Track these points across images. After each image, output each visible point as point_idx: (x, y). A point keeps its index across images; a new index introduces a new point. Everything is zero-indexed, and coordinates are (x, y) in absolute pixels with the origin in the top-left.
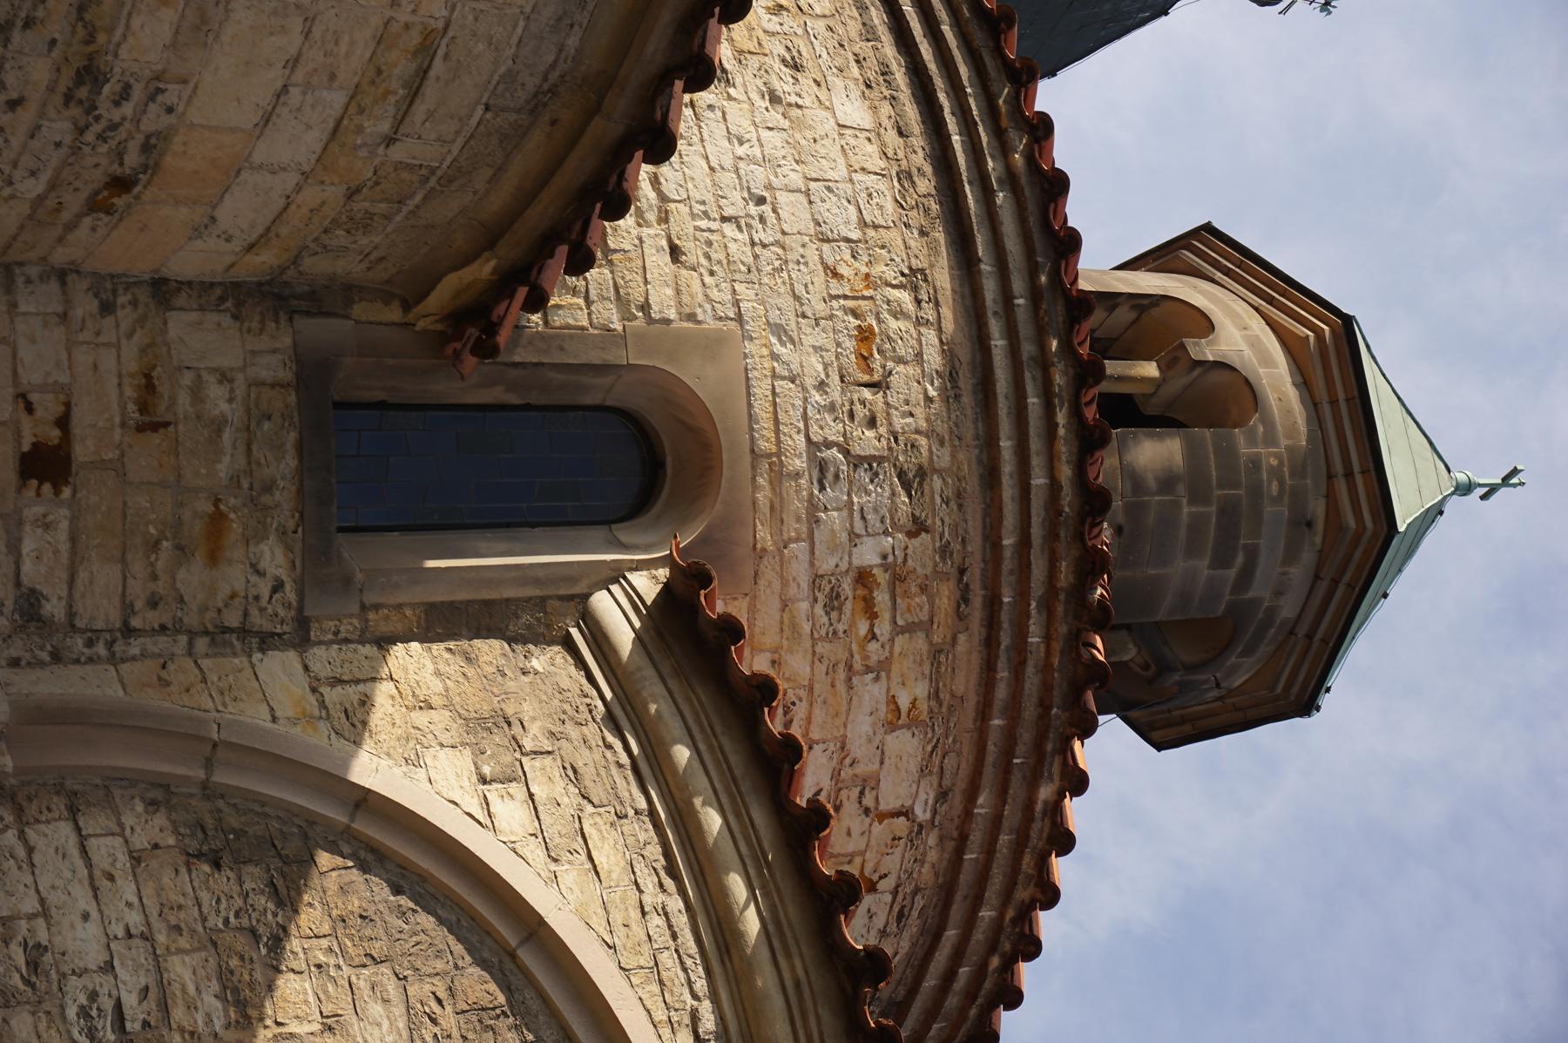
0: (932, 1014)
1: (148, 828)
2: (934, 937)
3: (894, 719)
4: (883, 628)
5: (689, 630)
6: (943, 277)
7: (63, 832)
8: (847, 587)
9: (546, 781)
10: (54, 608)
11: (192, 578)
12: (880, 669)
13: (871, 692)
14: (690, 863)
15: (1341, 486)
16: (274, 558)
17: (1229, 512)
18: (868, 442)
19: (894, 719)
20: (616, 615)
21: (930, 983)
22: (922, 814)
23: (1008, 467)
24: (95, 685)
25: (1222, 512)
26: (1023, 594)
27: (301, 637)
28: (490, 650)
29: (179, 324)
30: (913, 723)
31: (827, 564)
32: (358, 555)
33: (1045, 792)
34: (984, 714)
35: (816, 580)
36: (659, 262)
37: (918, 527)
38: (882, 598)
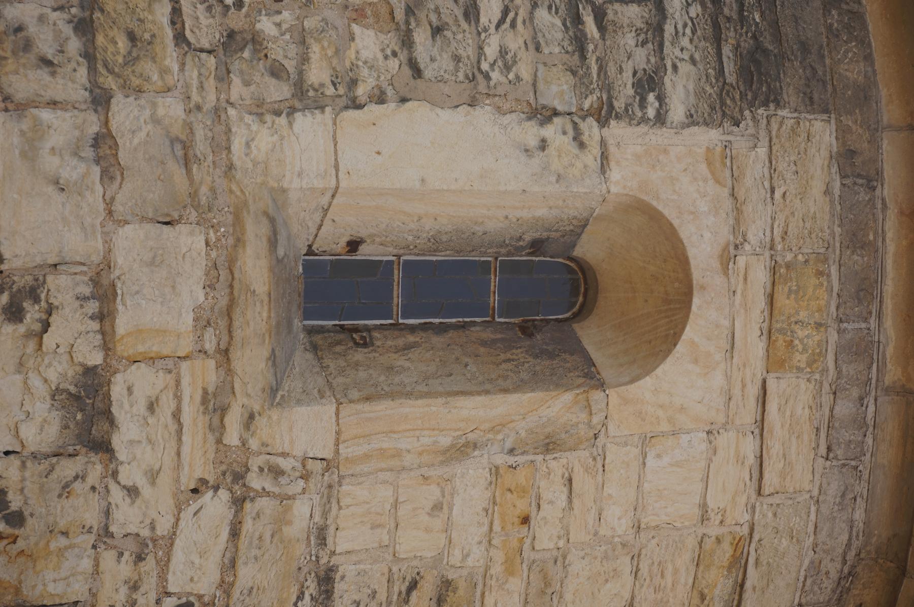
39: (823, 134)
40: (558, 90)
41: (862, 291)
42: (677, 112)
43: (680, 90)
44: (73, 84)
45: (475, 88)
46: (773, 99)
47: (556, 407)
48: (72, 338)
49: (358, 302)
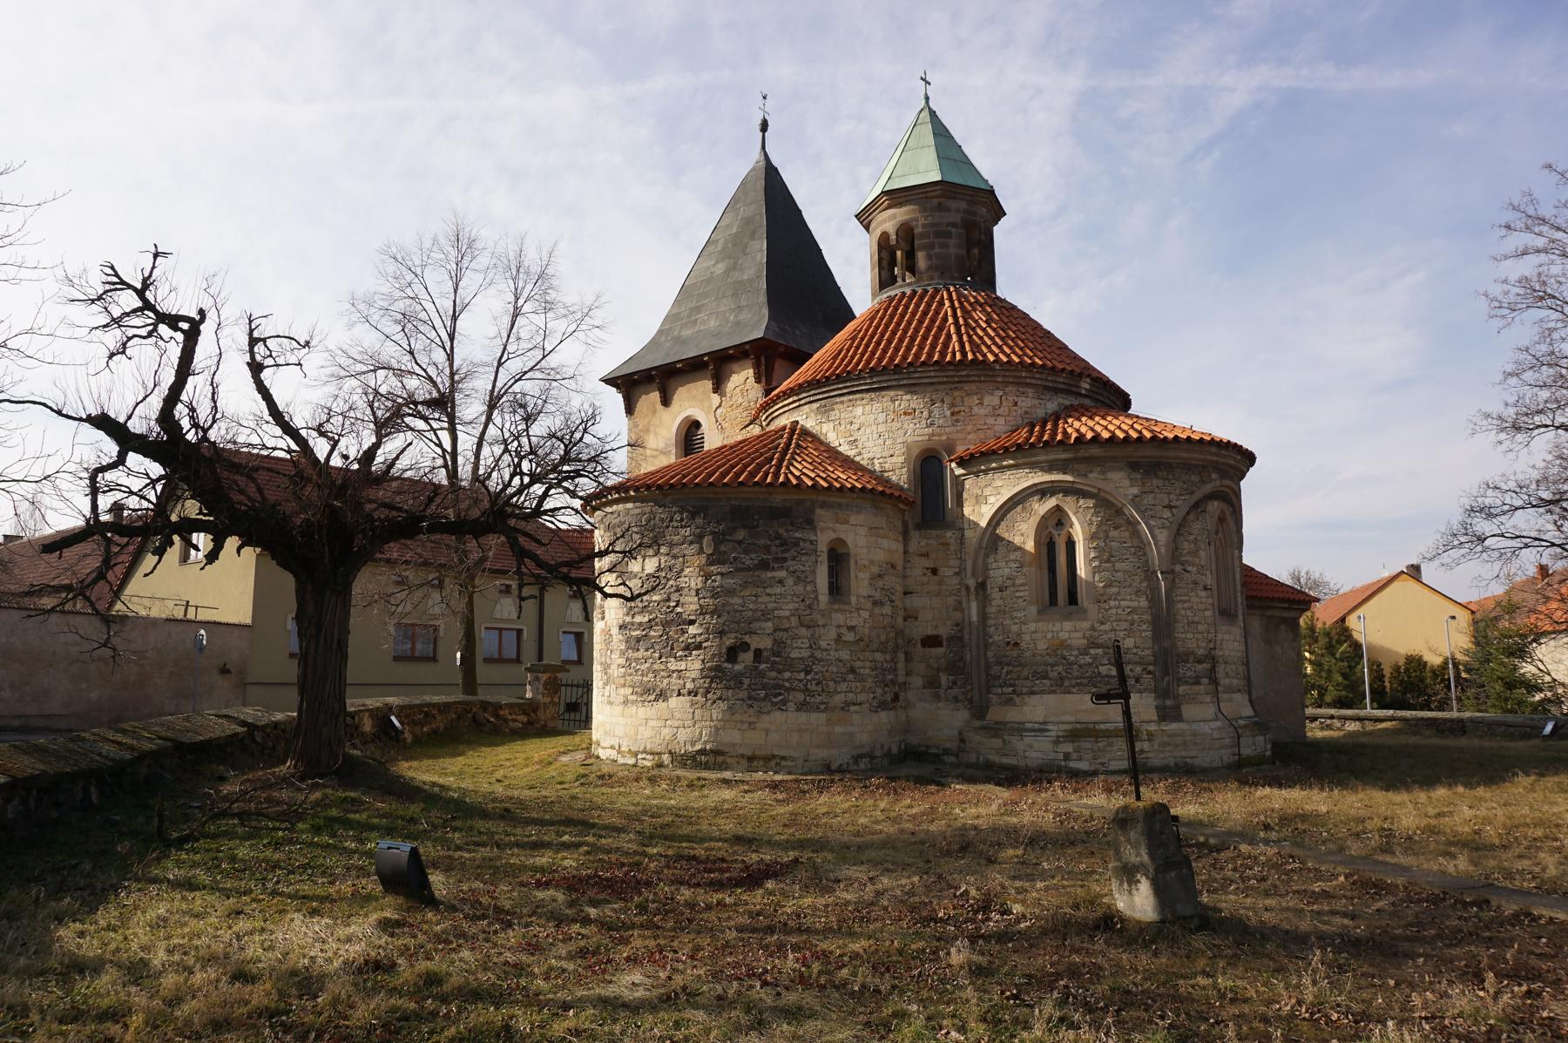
1: (991, 559)
3: (981, 404)
5: (962, 462)
6: (892, 393)
9: (987, 492)
11: (952, 548)
13: (976, 410)
14: (1001, 469)
16: (949, 534)
17: (938, 234)
18: (926, 414)
19: (981, 404)
20: (959, 471)
24: (969, 564)
28: (965, 495)
30: (981, 399)
32: (949, 518)
36: (894, 459)
39: (818, 511)
40: (813, 558)
41: (840, 505)
45: (814, 572)
48: (844, 630)
49: (837, 589)
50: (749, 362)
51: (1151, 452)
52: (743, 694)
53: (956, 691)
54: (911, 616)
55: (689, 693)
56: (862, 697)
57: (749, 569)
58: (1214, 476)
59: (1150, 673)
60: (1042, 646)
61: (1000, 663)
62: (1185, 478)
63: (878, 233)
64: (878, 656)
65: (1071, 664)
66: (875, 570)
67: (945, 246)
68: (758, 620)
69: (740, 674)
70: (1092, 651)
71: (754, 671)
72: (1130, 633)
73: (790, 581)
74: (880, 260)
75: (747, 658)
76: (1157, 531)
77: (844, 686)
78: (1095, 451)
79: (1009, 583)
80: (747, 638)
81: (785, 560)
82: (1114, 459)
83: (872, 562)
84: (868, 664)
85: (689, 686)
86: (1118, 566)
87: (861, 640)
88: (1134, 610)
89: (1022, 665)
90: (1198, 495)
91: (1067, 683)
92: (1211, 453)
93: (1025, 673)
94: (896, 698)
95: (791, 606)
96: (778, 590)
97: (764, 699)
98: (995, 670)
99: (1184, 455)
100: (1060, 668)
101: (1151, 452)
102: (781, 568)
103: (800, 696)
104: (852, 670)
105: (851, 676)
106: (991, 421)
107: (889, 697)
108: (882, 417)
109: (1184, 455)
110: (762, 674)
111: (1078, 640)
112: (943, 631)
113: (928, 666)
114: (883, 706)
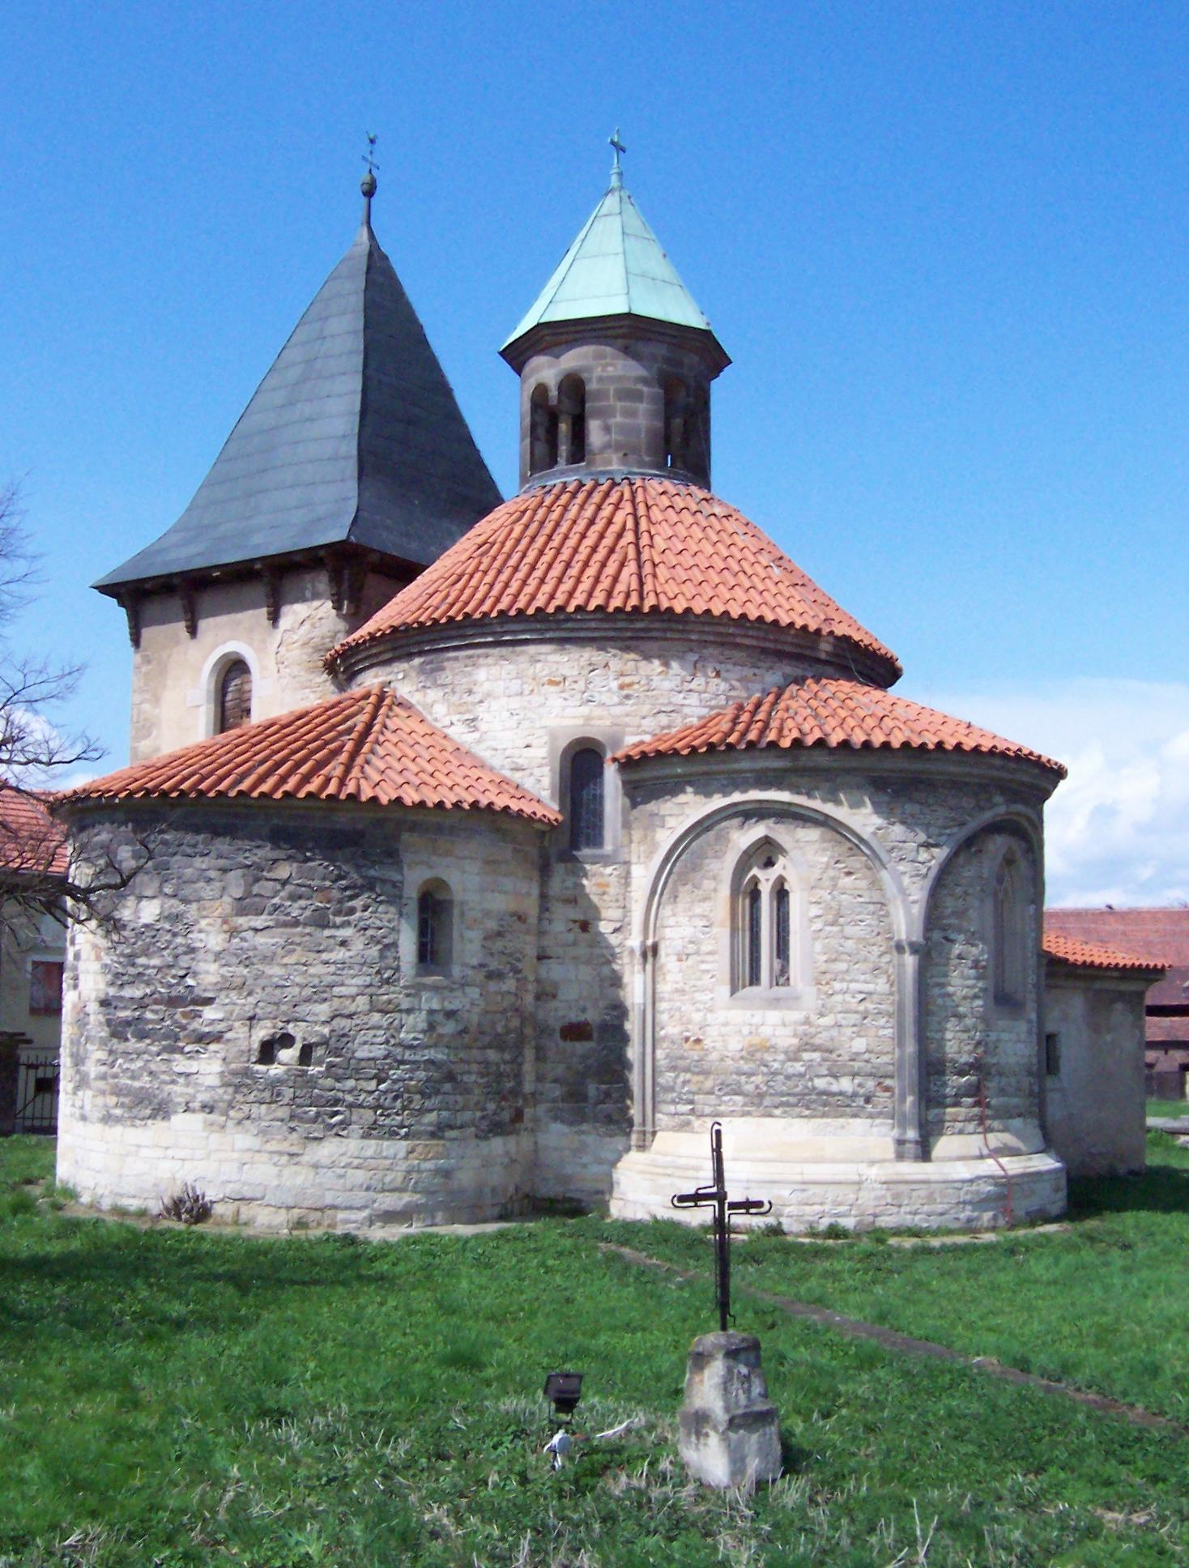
0: (765, 639)
2: (737, 646)
4: (635, 679)
7: (668, 930)
8: (625, 692)
10: (618, 925)
11: (612, 890)
12: (649, 679)
15: (609, 332)
16: (609, 870)
18: (581, 685)
21: (754, 643)
22: (695, 657)
23: (590, 635)
25: (620, 399)
26: (627, 629)
27: (627, 863)
29: (551, 893)
31: (616, 699)
33: (692, 618)
34: (666, 639)
35: (621, 704)
37: (606, 665)
38: (627, 680)
39: (405, 836)
42: (399, 878)
43: (396, 877)
44: (397, 1015)
46: (397, 850)
47: (456, 912)
48: (439, 1018)
50: (322, 582)
51: (902, 764)
52: (283, 1113)
53: (608, 1107)
54: (545, 994)
55: (204, 1107)
56: (467, 1116)
57: (296, 923)
58: (998, 799)
59: (887, 1089)
60: (735, 1045)
61: (673, 1068)
62: (953, 802)
63: (532, 384)
64: (492, 1055)
65: (775, 1074)
66: (492, 925)
67: (631, 414)
68: (308, 1000)
69: (279, 1081)
70: (806, 1056)
71: (301, 1080)
72: (860, 1030)
73: (358, 945)
74: (534, 426)
75: (288, 1055)
76: (906, 880)
77: (435, 1101)
78: (822, 759)
79: (691, 948)
80: (291, 1029)
81: (352, 911)
82: (848, 771)
83: (487, 914)
84: (474, 1067)
85: (203, 1097)
86: (850, 930)
87: (465, 1031)
88: (867, 996)
89: (706, 1073)
90: (974, 824)
91: (767, 1101)
92: (993, 767)
93: (709, 1084)
94: (518, 1116)
95: (359, 981)
96: (340, 954)
97: (314, 1120)
98: (666, 1078)
99: (952, 769)
100: (758, 1079)
101: (902, 764)
102: (347, 924)
103: (369, 1116)
104: (451, 1077)
105: (447, 1087)
106: (678, 699)
107: (506, 1116)
108: (515, 685)
109: (952, 769)
110: (312, 1082)
111: (786, 1039)
112: (592, 1016)
113: (569, 1068)
114: (497, 1128)
